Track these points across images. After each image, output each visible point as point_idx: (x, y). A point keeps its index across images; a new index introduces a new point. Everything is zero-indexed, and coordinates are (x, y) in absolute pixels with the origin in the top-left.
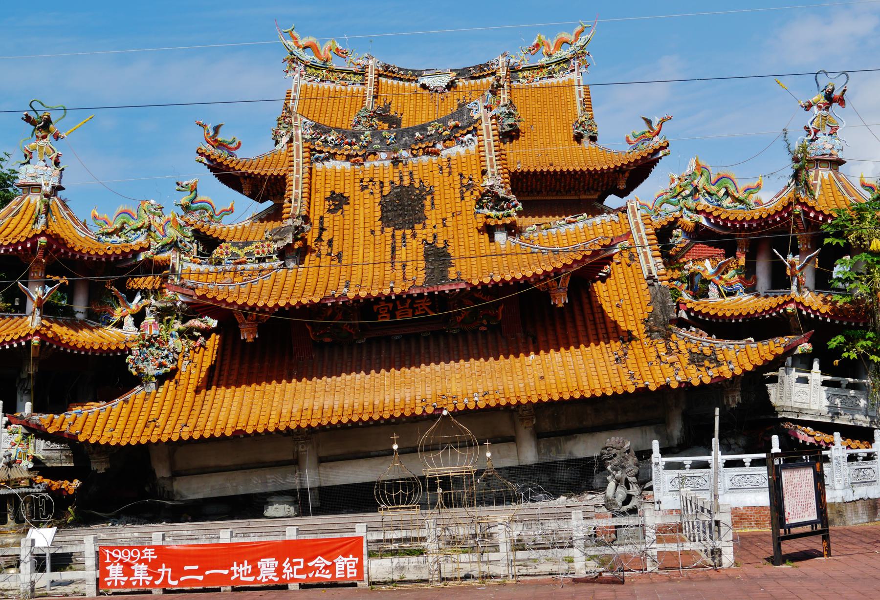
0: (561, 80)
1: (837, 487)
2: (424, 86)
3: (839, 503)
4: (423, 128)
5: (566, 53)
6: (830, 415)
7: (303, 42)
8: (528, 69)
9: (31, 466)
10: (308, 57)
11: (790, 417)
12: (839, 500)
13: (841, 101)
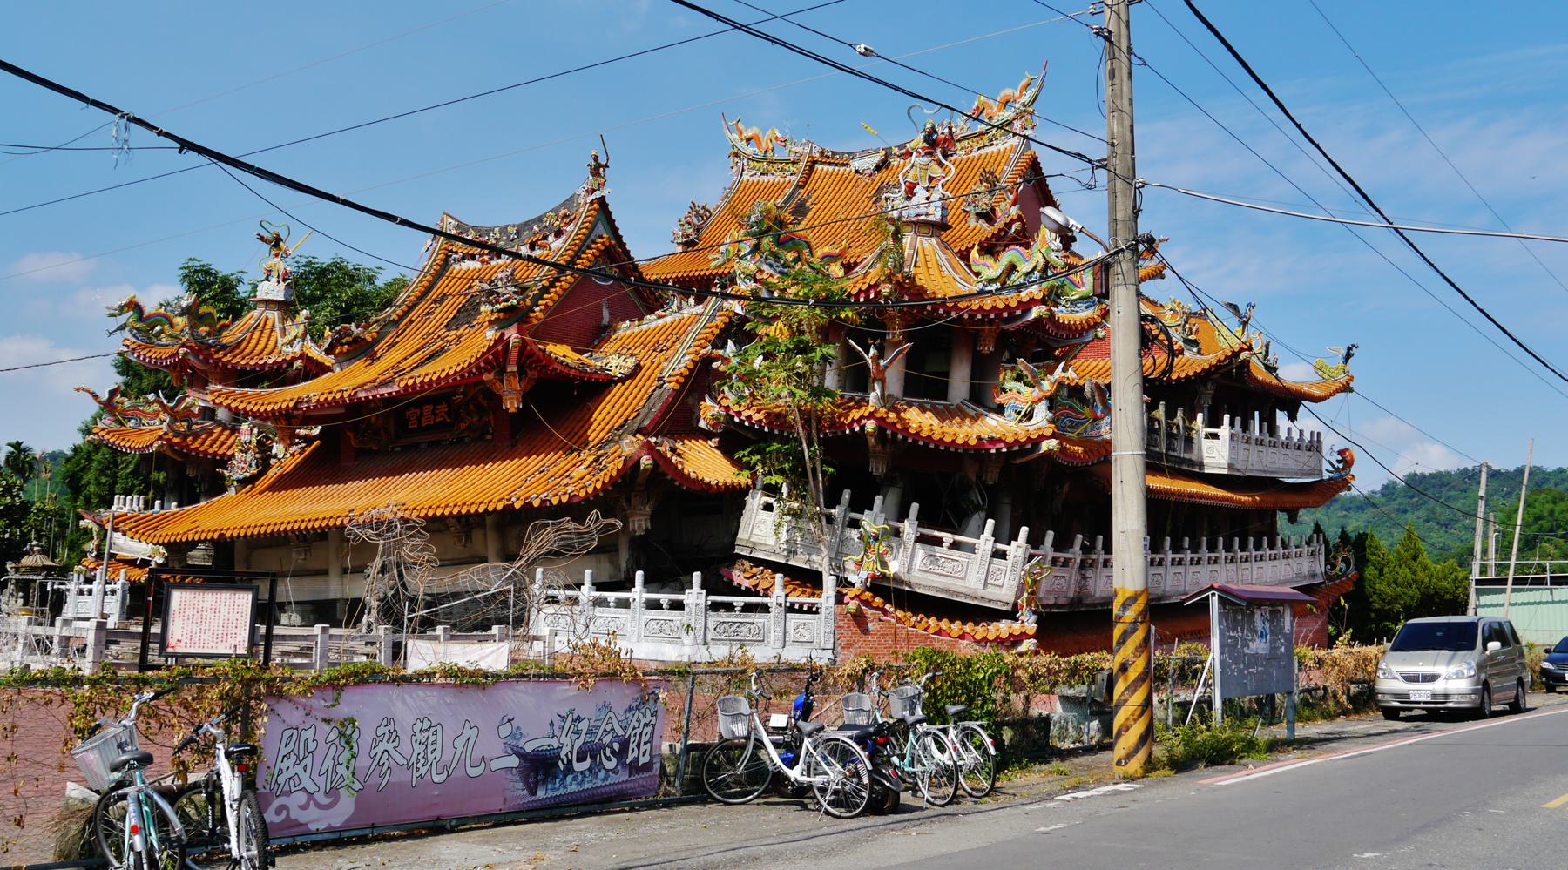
0: (1002, 148)
2: (857, 171)
4: (539, 220)
5: (1008, 114)
7: (748, 133)
8: (967, 138)
9: (160, 561)
10: (750, 150)
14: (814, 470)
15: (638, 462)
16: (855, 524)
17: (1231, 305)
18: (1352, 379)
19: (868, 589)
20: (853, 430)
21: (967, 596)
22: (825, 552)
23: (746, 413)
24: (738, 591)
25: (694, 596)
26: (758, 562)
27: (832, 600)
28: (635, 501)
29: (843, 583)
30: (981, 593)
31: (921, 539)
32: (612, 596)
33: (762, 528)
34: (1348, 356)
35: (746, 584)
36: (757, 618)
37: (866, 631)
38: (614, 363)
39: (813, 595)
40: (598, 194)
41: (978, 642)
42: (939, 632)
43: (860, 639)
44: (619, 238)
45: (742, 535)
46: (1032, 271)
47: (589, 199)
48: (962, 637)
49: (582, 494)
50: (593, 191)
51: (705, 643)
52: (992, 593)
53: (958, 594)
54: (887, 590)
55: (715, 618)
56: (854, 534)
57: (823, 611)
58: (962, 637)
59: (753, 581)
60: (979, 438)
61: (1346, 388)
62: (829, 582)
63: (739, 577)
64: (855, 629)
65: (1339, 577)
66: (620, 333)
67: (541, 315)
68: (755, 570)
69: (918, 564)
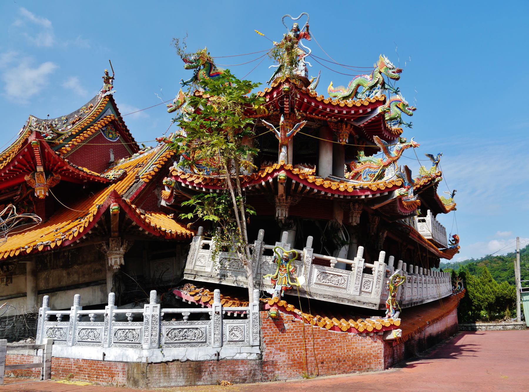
1: (145, 346)
3: (144, 363)
4: (78, 111)
6: (219, 277)
11: (189, 279)
12: (144, 360)
13: (306, 35)
14: (240, 213)
15: (108, 209)
16: (269, 253)
17: (429, 155)
18: (455, 204)
19: (282, 298)
20: (267, 182)
21: (349, 300)
22: (249, 272)
23: (190, 180)
24: (186, 305)
25: (151, 309)
26: (199, 285)
27: (257, 308)
28: (112, 244)
29: (264, 295)
30: (358, 298)
31: (316, 262)
32: (92, 313)
33: (203, 261)
34: (453, 195)
35: (191, 300)
36: (199, 324)
37: (283, 330)
38: (111, 174)
39: (241, 305)
40: (108, 93)
41: (360, 334)
42: (333, 328)
43: (279, 335)
44: (118, 114)
45: (189, 267)
46: (375, 85)
47: (104, 95)
48: (349, 330)
49: (70, 238)
50: (106, 91)
51: (160, 347)
52: (364, 298)
53: (343, 299)
54: (294, 298)
55: (167, 326)
56: (269, 259)
57: (251, 317)
58: (349, 330)
59: (197, 298)
60: (354, 188)
61: (454, 209)
62: (254, 295)
63: (186, 295)
64: (275, 329)
65: (458, 291)
66: (119, 165)
67: (69, 149)
68: (197, 290)
69: (314, 279)
